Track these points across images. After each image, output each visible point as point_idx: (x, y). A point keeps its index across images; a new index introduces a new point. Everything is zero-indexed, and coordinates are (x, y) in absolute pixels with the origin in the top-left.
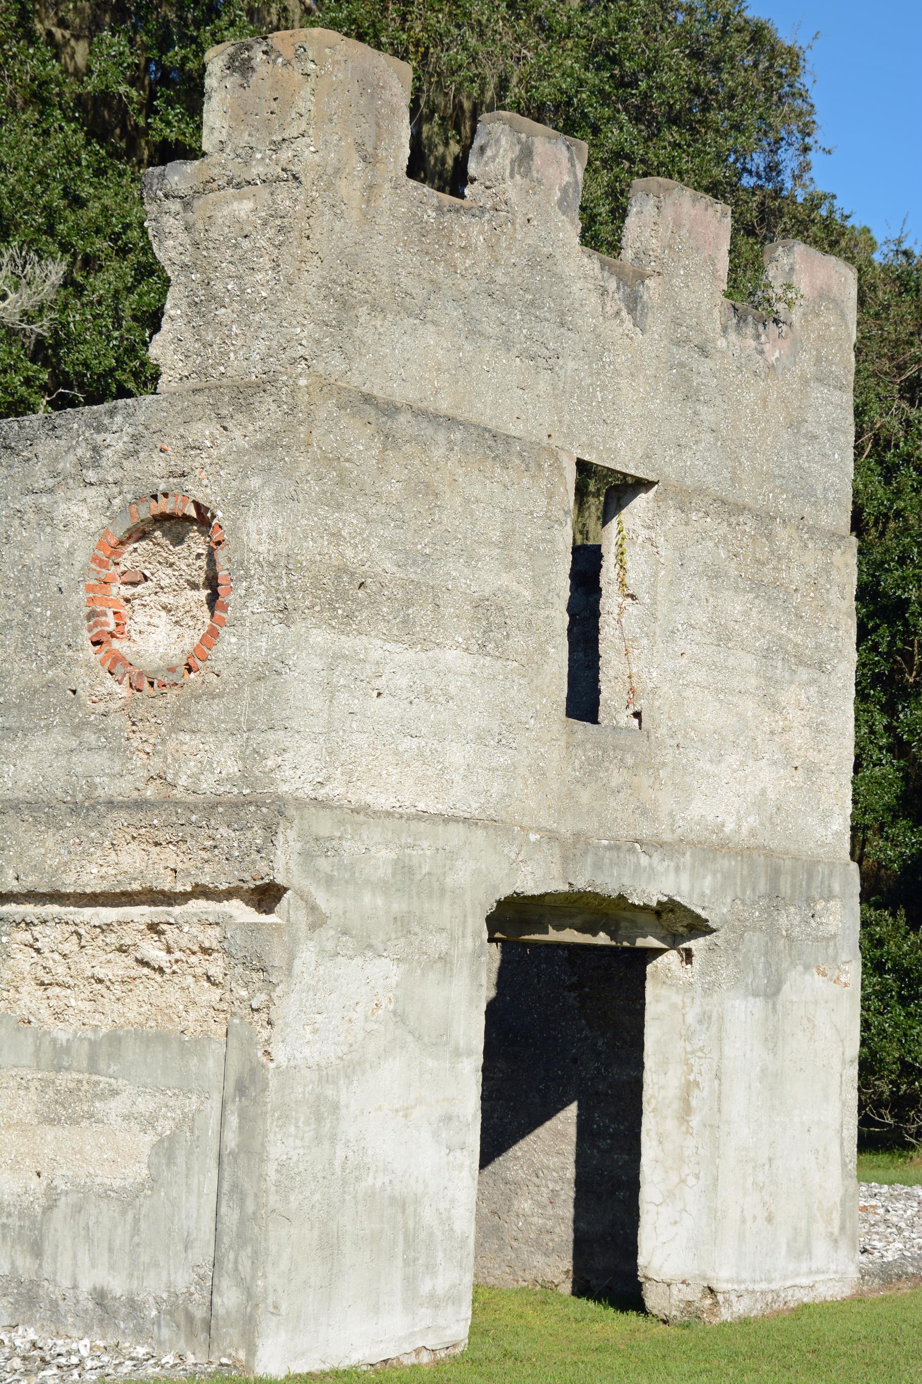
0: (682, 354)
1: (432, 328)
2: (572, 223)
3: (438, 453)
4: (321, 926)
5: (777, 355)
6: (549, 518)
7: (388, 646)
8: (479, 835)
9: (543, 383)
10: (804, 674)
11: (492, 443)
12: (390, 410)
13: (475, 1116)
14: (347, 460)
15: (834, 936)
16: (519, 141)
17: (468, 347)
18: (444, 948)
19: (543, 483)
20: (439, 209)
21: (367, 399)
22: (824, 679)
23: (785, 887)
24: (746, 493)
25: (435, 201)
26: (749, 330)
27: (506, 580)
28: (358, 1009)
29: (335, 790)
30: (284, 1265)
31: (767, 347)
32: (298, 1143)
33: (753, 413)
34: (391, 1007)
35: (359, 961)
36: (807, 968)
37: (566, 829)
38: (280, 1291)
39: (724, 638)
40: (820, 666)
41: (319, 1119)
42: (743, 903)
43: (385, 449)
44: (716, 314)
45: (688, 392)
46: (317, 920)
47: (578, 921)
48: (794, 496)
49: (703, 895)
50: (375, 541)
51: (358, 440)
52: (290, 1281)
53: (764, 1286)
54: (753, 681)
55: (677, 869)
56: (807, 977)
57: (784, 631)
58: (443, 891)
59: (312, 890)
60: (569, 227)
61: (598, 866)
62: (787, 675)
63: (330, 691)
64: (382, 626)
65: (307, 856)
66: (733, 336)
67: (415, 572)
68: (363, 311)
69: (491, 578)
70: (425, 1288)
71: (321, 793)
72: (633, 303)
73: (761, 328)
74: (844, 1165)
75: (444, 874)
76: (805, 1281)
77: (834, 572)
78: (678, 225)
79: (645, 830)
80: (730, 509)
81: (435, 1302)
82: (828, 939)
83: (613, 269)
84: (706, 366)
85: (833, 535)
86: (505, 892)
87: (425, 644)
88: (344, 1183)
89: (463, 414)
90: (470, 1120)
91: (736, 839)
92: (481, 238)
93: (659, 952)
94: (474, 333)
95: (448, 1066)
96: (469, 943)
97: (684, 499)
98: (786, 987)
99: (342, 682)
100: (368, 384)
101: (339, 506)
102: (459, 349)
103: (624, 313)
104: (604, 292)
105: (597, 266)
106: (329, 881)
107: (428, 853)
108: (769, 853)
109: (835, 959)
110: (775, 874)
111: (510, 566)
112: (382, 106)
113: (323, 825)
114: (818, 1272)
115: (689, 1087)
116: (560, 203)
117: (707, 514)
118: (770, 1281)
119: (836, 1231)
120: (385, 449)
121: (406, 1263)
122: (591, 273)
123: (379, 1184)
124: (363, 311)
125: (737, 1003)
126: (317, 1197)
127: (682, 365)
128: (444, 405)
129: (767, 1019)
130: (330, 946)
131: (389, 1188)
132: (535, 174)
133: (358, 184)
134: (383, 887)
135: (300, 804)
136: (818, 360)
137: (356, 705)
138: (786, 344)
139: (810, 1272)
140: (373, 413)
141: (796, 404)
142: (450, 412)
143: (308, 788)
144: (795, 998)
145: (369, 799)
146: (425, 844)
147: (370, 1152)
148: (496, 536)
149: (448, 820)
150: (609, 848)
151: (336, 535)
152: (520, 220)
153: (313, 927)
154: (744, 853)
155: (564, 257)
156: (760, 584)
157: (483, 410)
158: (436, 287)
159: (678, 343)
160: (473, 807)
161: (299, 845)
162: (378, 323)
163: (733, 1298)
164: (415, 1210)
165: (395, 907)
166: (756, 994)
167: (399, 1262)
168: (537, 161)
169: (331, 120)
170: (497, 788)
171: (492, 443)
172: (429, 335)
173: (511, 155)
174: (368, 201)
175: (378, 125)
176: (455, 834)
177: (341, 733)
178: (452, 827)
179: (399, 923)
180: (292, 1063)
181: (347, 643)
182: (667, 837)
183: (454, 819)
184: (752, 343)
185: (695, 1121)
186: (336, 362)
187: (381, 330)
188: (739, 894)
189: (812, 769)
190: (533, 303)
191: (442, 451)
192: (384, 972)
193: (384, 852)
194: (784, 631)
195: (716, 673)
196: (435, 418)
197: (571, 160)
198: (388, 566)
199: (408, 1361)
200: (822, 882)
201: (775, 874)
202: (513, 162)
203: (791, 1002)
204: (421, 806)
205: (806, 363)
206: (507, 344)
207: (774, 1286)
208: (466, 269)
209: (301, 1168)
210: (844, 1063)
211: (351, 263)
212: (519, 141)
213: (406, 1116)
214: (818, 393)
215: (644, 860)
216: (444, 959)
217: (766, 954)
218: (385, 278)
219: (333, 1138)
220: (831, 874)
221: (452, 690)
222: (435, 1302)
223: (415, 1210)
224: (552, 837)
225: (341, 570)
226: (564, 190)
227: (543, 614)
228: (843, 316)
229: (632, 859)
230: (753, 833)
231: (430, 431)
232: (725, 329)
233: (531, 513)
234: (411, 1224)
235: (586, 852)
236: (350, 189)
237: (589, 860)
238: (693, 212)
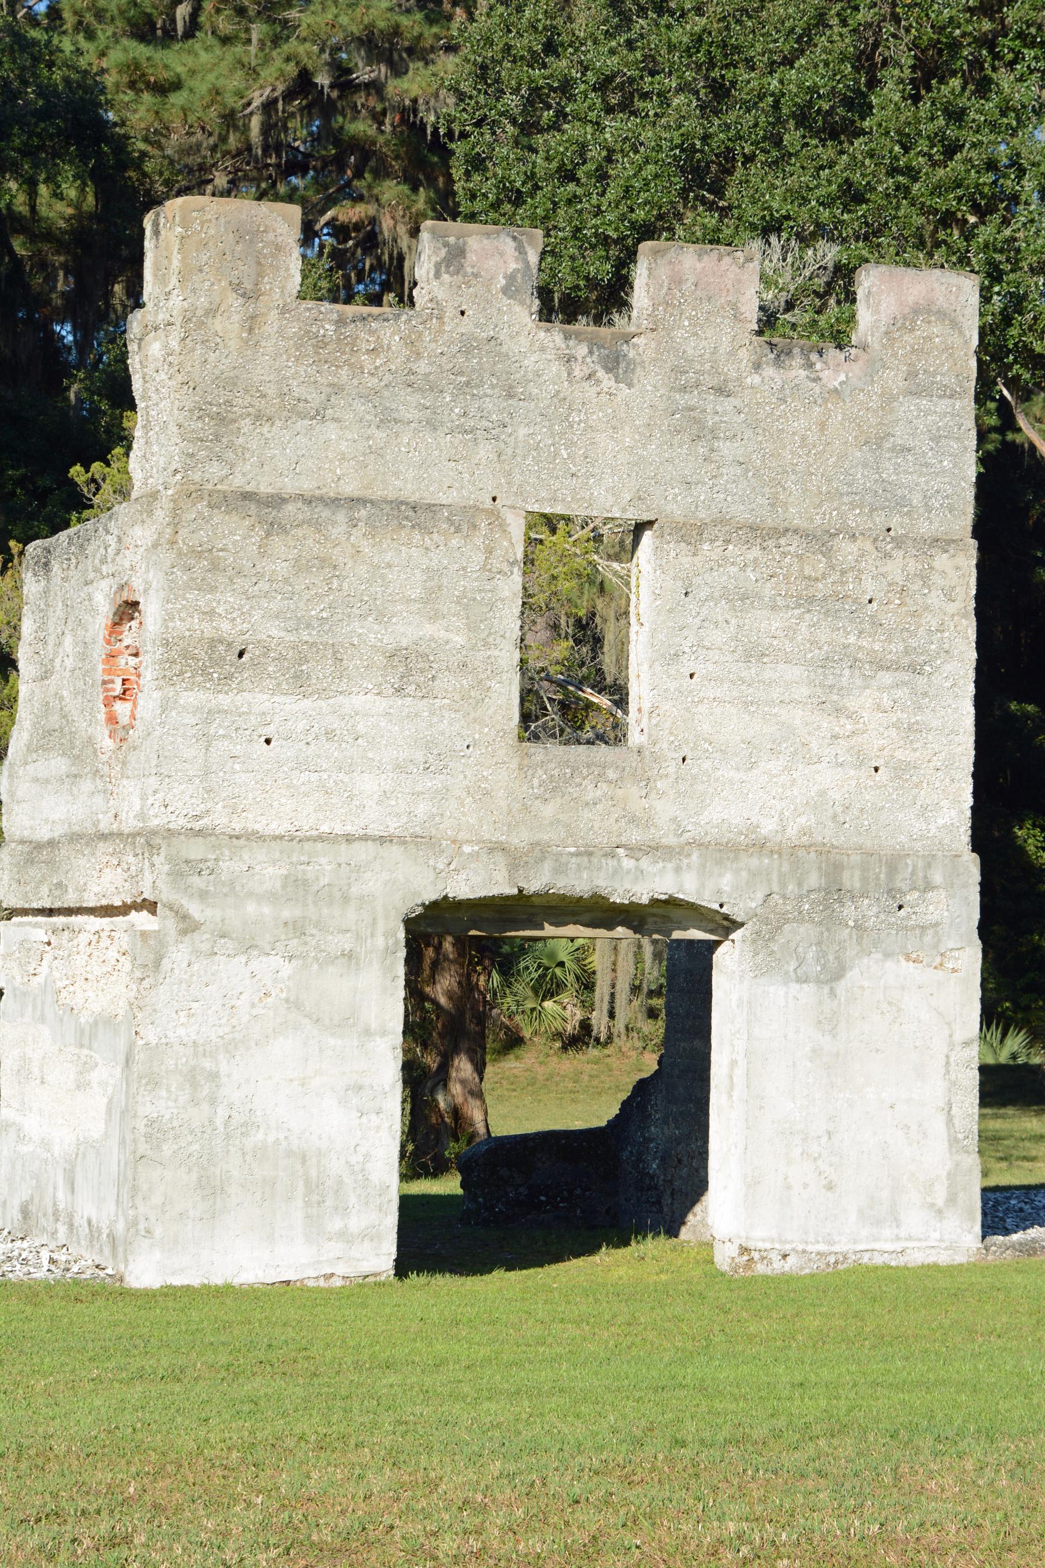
0: (692, 399)
1: (333, 425)
2: (522, 303)
3: (338, 531)
4: (193, 931)
5: (842, 377)
6: (490, 570)
7: (276, 699)
8: (394, 851)
9: (485, 451)
10: (886, 678)
11: (413, 514)
12: (277, 501)
13: (393, 1086)
14: (222, 550)
15: (937, 925)
16: (446, 245)
17: (380, 435)
18: (347, 947)
19: (479, 541)
20: (341, 322)
21: (247, 496)
22: (922, 681)
23: (851, 880)
24: (795, 516)
25: (335, 316)
26: (798, 360)
27: (429, 629)
28: (242, 997)
29: (219, 819)
30: (157, 1199)
31: (825, 374)
32: (171, 1104)
33: (804, 439)
34: (284, 995)
35: (243, 959)
36: (887, 955)
37: (520, 839)
38: (153, 1219)
39: (755, 654)
40: (915, 669)
41: (195, 1085)
42: (784, 897)
43: (268, 534)
44: (743, 354)
45: (700, 432)
46: (188, 926)
47: (586, 917)
48: (872, 510)
49: (719, 892)
50: (257, 615)
51: (235, 533)
52: (164, 1212)
53: (822, 1247)
54: (805, 691)
55: (678, 870)
56: (889, 964)
57: (852, 639)
58: (346, 899)
59: (183, 902)
60: (517, 308)
61: (560, 869)
62: (859, 682)
63: (207, 740)
64: (270, 684)
65: (177, 875)
66: (769, 371)
67: (310, 634)
68: (246, 425)
69: (409, 629)
70: (336, 1224)
71: (197, 826)
72: (614, 363)
73: (814, 357)
74: (953, 1141)
75: (349, 884)
76: (889, 1247)
77: (935, 578)
78: (677, 281)
79: (635, 836)
80: (756, 533)
81: (344, 1236)
82: (923, 928)
83: (582, 337)
84: (727, 404)
85: (941, 543)
86: (431, 895)
87: (322, 693)
88: (228, 1137)
89: (377, 493)
90: (387, 1089)
91: (779, 838)
92: (397, 338)
93: (718, 943)
94: (387, 420)
95: (356, 1044)
96: (380, 942)
97: (691, 533)
98: (853, 975)
99: (221, 732)
100: (253, 483)
101: (213, 589)
102: (368, 438)
103: (601, 374)
104: (569, 359)
105: (558, 338)
106: (203, 895)
107: (328, 868)
108: (823, 851)
109: (935, 947)
110: (833, 870)
111: (435, 617)
112: (263, 247)
113: (195, 850)
114: (910, 1238)
115: (733, 1063)
116: (505, 290)
117: (728, 542)
118: (830, 1243)
119: (940, 1202)
120: (268, 534)
121: (307, 1204)
122: (551, 345)
123: (271, 1139)
124: (246, 425)
125: (772, 989)
126: (196, 1147)
127: (691, 409)
128: (350, 488)
129: (820, 1003)
130: (205, 947)
131: (284, 1144)
132: (469, 270)
133: (236, 318)
134: (272, 897)
135: (170, 833)
136: (911, 375)
137: (238, 750)
138: (856, 368)
139: (898, 1238)
140: (253, 507)
141: (873, 421)
142: (356, 494)
143: (182, 821)
144: (866, 984)
145: (257, 827)
146: (323, 861)
147: (258, 1113)
148: (416, 593)
149: (349, 839)
150: (577, 854)
151: (211, 614)
152: (450, 312)
153: (184, 932)
154: (792, 853)
155: (512, 337)
156: (811, 600)
157: (406, 486)
158: (337, 389)
159: (684, 389)
160: (393, 826)
161: (167, 867)
162: (265, 429)
163: (775, 1256)
164: (319, 1162)
165: (286, 914)
166: (802, 980)
167: (300, 1203)
168: (471, 257)
169: (201, 271)
170: (422, 809)
171: (413, 514)
172: (331, 431)
173: (435, 259)
174: (251, 330)
175: (259, 263)
176: (363, 852)
177: (221, 774)
178: (356, 845)
179: (291, 927)
180: (163, 1041)
181: (224, 700)
182: (671, 840)
183: (365, 838)
184: (803, 373)
185: (736, 1094)
186: (215, 470)
187: (269, 436)
188: (775, 888)
189: (901, 770)
190: (468, 384)
191: (344, 527)
192: (273, 968)
193: (271, 869)
194: (852, 639)
195: (744, 687)
196: (335, 502)
197: (521, 250)
198: (274, 632)
199: (311, 1283)
200: (913, 873)
201: (833, 870)
202: (438, 266)
203: (862, 988)
204: (325, 828)
205: (893, 379)
206: (432, 425)
207: (836, 1248)
208: (376, 368)
209: (175, 1123)
210: (952, 1046)
211: (231, 384)
212: (446, 245)
213: (303, 1085)
214: (907, 407)
215: (628, 863)
216: (349, 956)
217: (819, 944)
218: (271, 391)
219: (213, 1101)
220: (929, 865)
221: (361, 728)
222: (344, 1236)
223: (319, 1162)
224: (503, 849)
225: (213, 643)
226: (511, 278)
227: (480, 655)
228: (955, 324)
229: (612, 863)
230: (804, 832)
231: (326, 513)
232: (757, 366)
233: (464, 569)
234: (313, 1173)
235: (542, 859)
236: (229, 325)
237: (547, 866)
238: (699, 266)
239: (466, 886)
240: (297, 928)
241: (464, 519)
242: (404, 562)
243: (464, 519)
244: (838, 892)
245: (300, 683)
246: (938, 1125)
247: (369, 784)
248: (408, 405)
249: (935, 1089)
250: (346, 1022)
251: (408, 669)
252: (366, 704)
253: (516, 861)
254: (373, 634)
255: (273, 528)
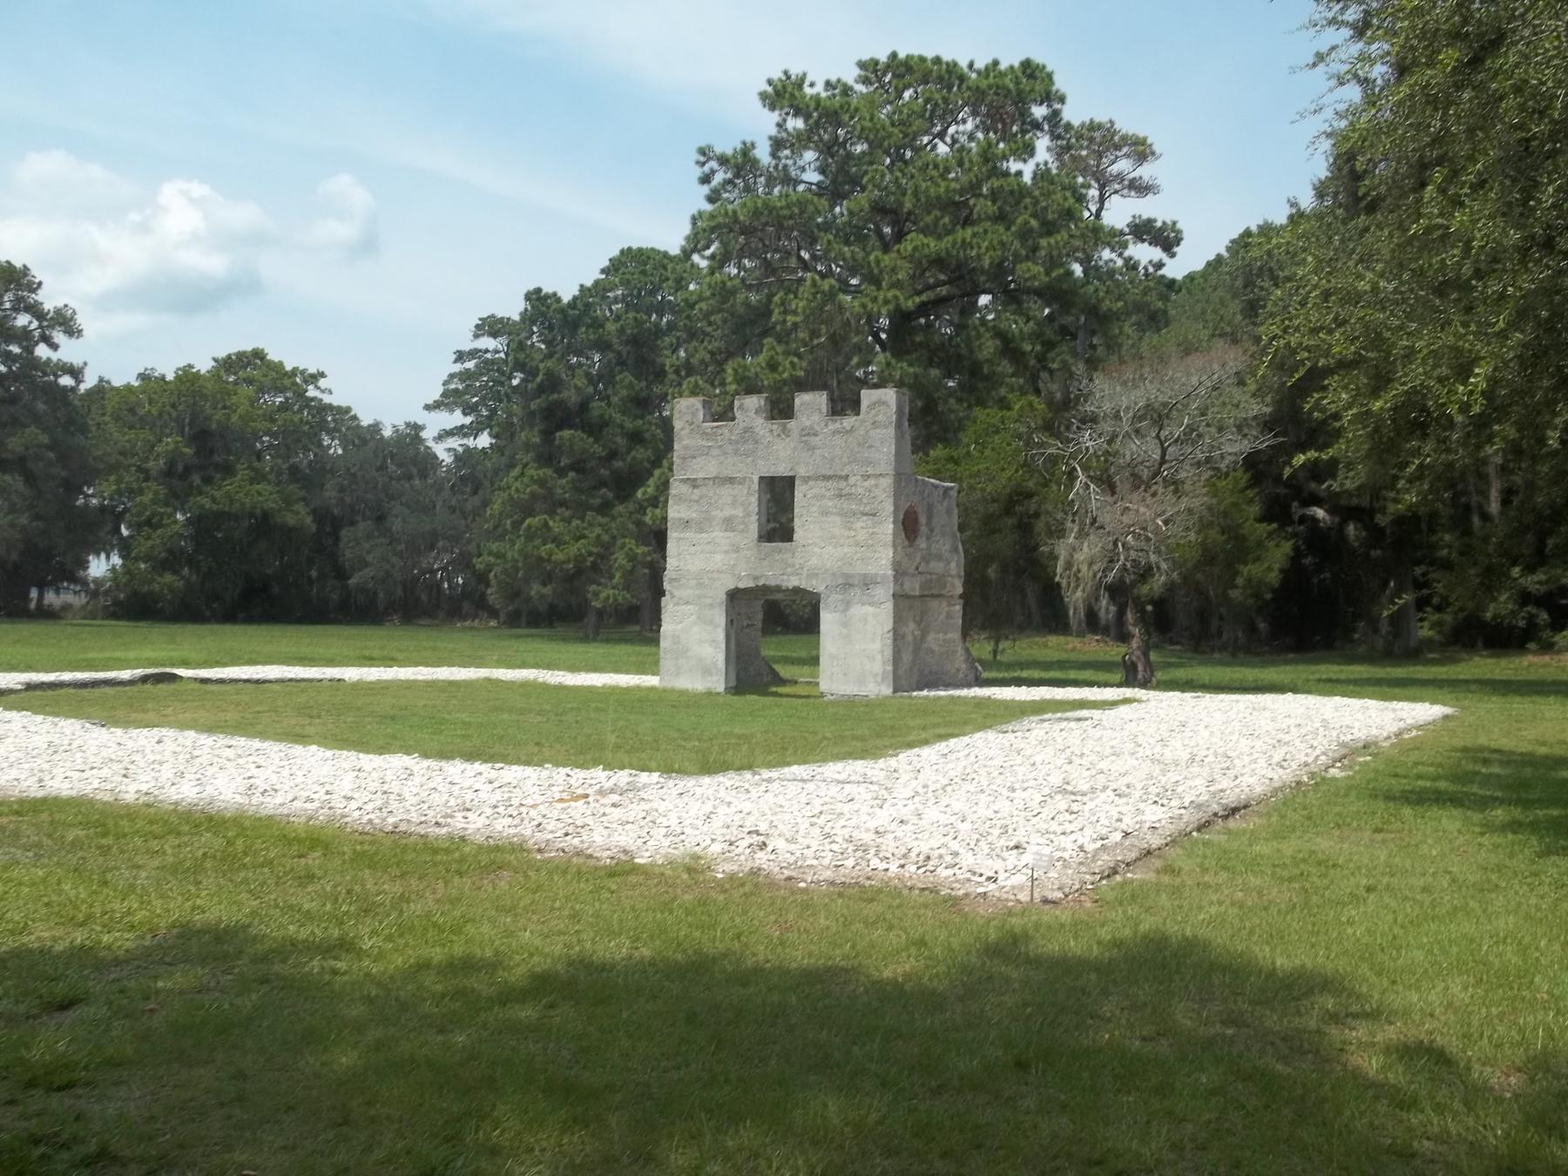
11: (731, 480)
39: (825, 513)
69: (728, 512)
80: (826, 478)
97: (806, 480)
157: (729, 472)
171: (731, 480)
214: (872, 433)
239: (741, 586)
240: (699, 597)
241: (742, 481)
242: (727, 492)
243: (742, 481)
244: (853, 584)
245: (701, 531)
246: (879, 657)
247: (718, 557)
248: (729, 449)
249: (877, 645)
250: (711, 622)
251: (729, 524)
252: (718, 535)
253: (756, 578)
254: (719, 514)
255: (695, 487)
